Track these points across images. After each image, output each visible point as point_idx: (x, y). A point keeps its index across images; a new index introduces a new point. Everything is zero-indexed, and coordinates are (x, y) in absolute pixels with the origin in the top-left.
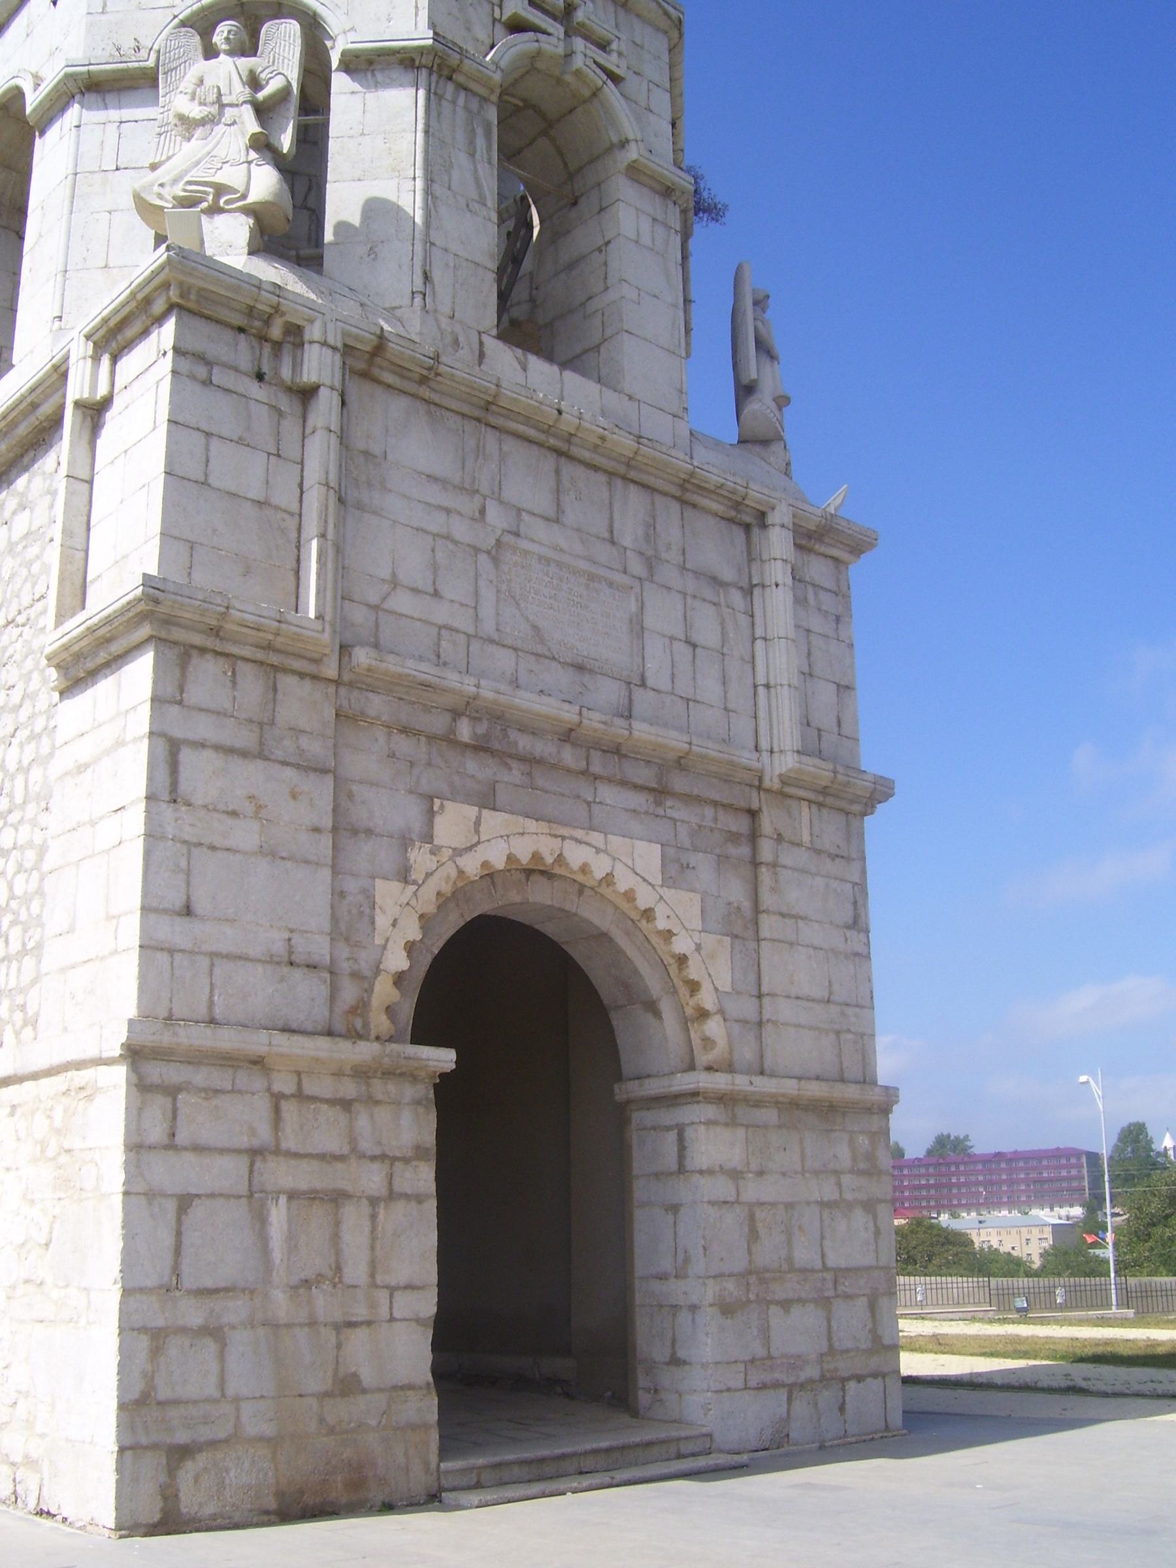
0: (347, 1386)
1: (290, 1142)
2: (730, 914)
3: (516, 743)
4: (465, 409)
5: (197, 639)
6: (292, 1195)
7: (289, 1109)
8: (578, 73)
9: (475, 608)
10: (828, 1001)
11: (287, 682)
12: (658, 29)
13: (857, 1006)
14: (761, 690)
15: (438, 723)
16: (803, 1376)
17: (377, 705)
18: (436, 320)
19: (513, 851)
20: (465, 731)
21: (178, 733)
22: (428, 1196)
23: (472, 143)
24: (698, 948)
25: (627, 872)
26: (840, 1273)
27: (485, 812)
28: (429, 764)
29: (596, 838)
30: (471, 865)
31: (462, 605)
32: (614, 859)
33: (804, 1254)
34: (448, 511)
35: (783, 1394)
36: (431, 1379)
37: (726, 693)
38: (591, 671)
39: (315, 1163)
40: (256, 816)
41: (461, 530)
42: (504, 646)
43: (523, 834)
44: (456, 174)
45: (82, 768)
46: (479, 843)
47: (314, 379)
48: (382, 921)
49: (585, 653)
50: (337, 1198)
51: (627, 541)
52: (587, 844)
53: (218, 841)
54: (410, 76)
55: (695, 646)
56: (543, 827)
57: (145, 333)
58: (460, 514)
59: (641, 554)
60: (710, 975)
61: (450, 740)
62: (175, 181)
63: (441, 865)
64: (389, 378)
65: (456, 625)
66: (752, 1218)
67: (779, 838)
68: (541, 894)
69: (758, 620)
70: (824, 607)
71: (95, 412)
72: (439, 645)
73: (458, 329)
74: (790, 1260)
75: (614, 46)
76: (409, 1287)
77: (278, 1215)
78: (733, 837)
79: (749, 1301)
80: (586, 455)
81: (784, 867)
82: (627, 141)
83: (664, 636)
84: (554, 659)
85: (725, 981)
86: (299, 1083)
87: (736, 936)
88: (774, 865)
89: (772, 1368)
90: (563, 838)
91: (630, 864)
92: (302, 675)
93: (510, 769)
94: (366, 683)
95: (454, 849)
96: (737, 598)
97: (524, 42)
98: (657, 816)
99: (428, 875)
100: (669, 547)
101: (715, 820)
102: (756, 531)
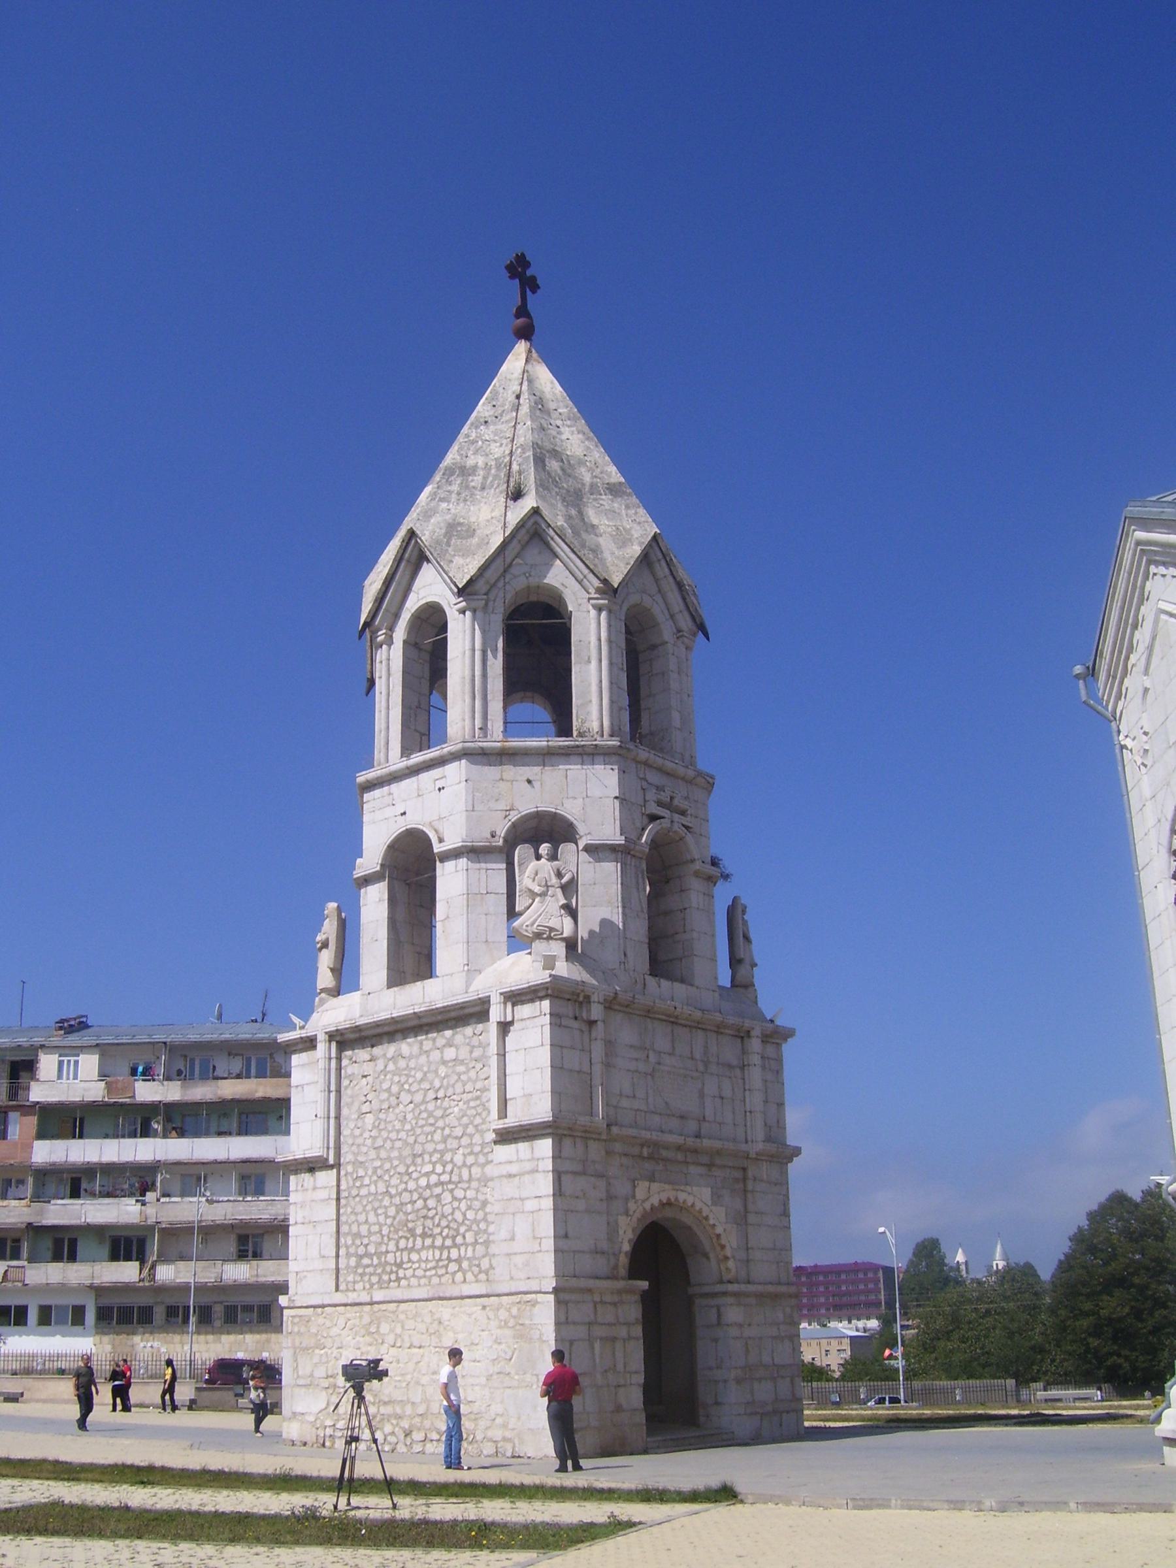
0: (619, 1409)
1: (600, 1320)
6: (601, 1339)
7: (599, 1307)
8: (675, 832)
11: (591, 1143)
15: (636, 1150)
17: (618, 1147)
20: (645, 1152)
23: (637, 883)
25: (699, 1199)
29: (688, 1188)
30: (647, 1206)
33: (766, 1359)
35: (759, 1417)
41: (642, 1067)
45: (510, 1176)
48: (621, 1232)
50: (614, 1339)
54: (613, 856)
56: (670, 1187)
57: (532, 1001)
61: (641, 1157)
62: (533, 924)
64: (617, 1007)
67: (755, 1179)
68: (669, 1213)
71: (505, 1027)
77: (597, 1345)
78: (736, 1180)
88: (752, 1191)
92: (594, 1140)
96: (738, 1072)
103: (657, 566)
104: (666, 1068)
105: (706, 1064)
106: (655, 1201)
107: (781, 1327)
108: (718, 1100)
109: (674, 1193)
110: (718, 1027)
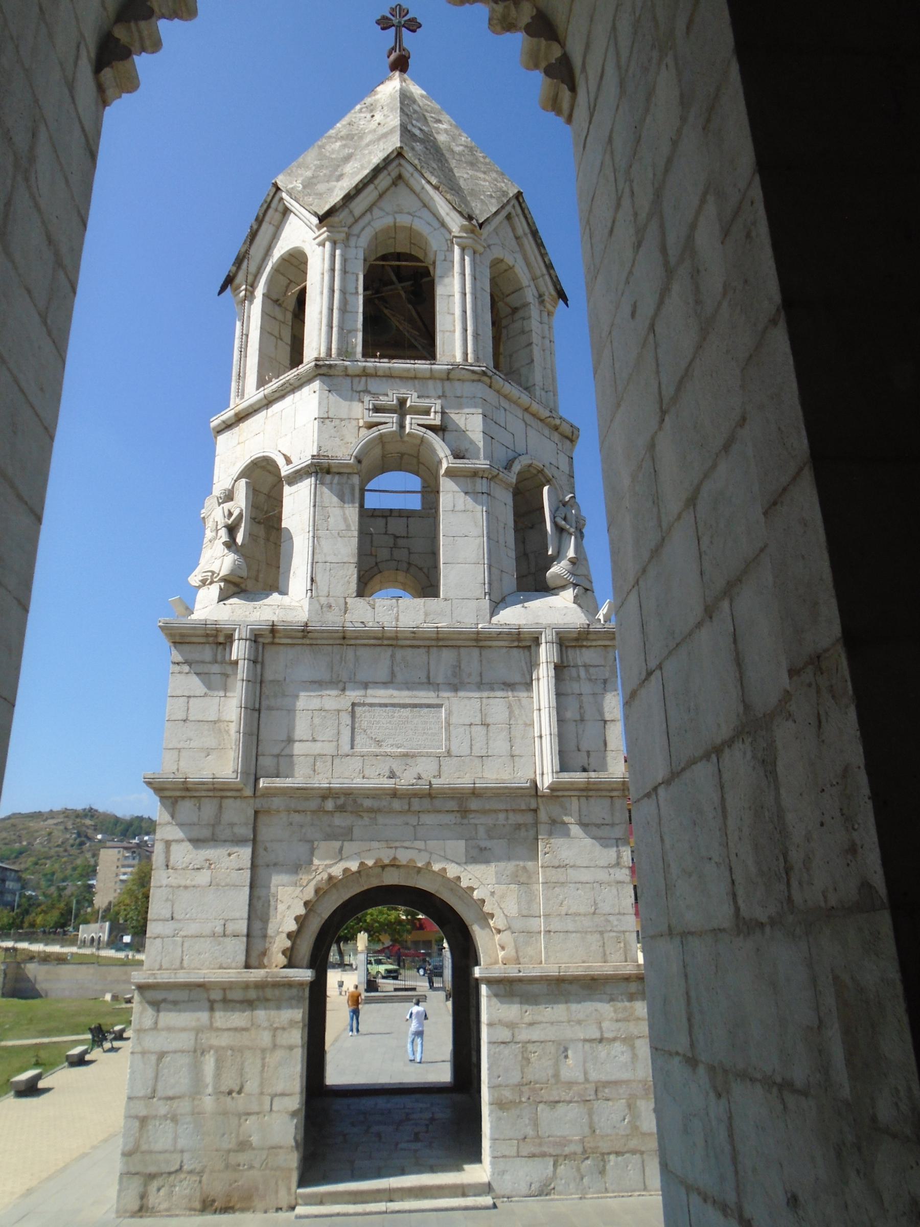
0: (243, 1145)
2: (517, 871)
3: (362, 805)
4: (331, 642)
5: (178, 794)
12: (473, 381)
13: (619, 914)
15: (313, 805)
16: (567, 1150)
18: (318, 601)
20: (330, 805)
21: (170, 838)
22: (296, 1047)
24: (493, 893)
26: (599, 1087)
27: (346, 843)
28: (312, 825)
29: (419, 844)
32: (431, 853)
36: (294, 1144)
37: (512, 747)
38: (413, 756)
39: (231, 1033)
40: (209, 868)
44: (331, 520)
51: (440, 680)
53: (188, 883)
55: (488, 725)
56: (384, 844)
66: (524, 1050)
70: (593, 677)
73: (331, 600)
74: (556, 1075)
75: (433, 410)
76: (283, 1095)
79: (521, 1102)
80: (408, 643)
86: (225, 994)
89: (540, 1145)
90: (396, 848)
91: (442, 854)
92: (235, 798)
93: (362, 817)
94: (270, 793)
100: (470, 675)
101: (507, 818)
102: (533, 648)
103: (412, 182)
108: (479, 731)
110: (477, 640)
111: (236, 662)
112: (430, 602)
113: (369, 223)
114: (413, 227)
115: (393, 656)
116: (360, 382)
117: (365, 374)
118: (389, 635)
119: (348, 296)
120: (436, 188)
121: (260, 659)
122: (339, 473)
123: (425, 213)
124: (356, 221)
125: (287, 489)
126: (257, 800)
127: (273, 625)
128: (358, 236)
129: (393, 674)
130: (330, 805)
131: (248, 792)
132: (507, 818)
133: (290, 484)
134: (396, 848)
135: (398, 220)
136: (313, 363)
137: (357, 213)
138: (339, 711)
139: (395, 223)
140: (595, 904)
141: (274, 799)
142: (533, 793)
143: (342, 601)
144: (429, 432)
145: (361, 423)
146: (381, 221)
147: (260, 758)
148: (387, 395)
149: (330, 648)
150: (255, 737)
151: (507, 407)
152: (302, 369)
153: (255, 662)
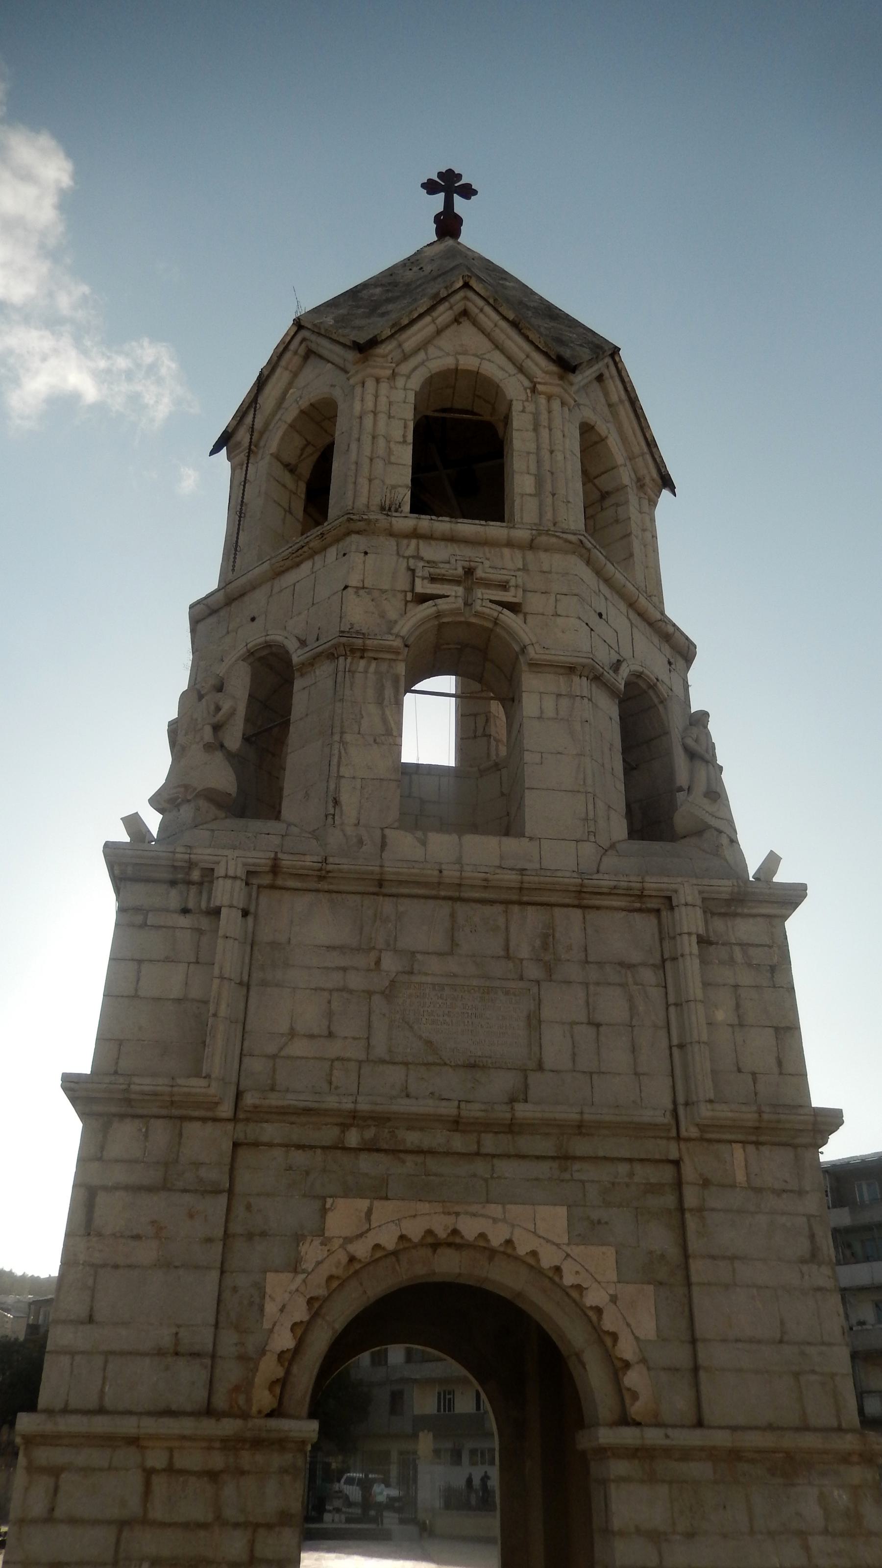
4: (360, 889)
8: (477, 614)
9: (368, 1038)
10: (781, 1341)
14: (676, 1051)
15: (329, 1135)
17: (270, 1131)
18: (343, 830)
19: (404, 1232)
20: (353, 1138)
24: (614, 1299)
27: (376, 1203)
29: (495, 1210)
30: (362, 1250)
31: (354, 1039)
32: (513, 1226)
34: (344, 969)
38: (484, 1067)
41: (355, 981)
42: (394, 1063)
43: (415, 1216)
46: (369, 1230)
47: (218, 904)
49: (479, 1054)
52: (482, 1216)
58: (357, 969)
59: (539, 960)
60: (628, 1325)
63: (331, 1252)
64: (291, 883)
65: (348, 1055)
67: (706, 1183)
69: (670, 989)
72: (331, 1075)
78: (651, 1189)
80: (477, 895)
81: (713, 1210)
82: (525, 647)
83: (563, 1023)
84: (445, 1064)
85: (647, 1328)
87: (661, 1283)
88: (700, 1210)
90: (457, 1214)
91: (531, 1227)
92: (204, 1120)
93: (404, 1162)
94: (259, 1114)
95: (345, 1238)
97: (427, 609)
98: (562, 1181)
99: (319, 1263)
103: (481, 318)
104: (429, 979)
105: (549, 969)
106: (388, 1239)
107: (817, 1542)
109: (449, 1221)
111: (215, 912)
112: (510, 844)
113: (423, 363)
114: (481, 371)
115: (453, 915)
116: (408, 546)
117: (415, 534)
118: (447, 881)
119: (392, 445)
120: (514, 324)
121: (252, 909)
122: (375, 659)
123: (497, 356)
124: (406, 358)
125: (298, 684)
126: (240, 1126)
127: (276, 859)
128: (408, 377)
129: (454, 943)
130: (353, 1138)
131: (226, 1110)
132: (631, 1175)
133: (302, 675)
134: (457, 1214)
135: (461, 362)
136: (346, 517)
137: (408, 346)
138: (370, 993)
139: (457, 365)
140: (782, 1323)
141: (265, 1125)
142: (673, 1133)
143: (378, 833)
144: (505, 611)
145: (409, 596)
146: (439, 360)
147: (246, 1060)
148: (449, 563)
149: (358, 898)
150: (240, 1027)
151: (608, 596)
152: (326, 526)
153: (245, 913)
